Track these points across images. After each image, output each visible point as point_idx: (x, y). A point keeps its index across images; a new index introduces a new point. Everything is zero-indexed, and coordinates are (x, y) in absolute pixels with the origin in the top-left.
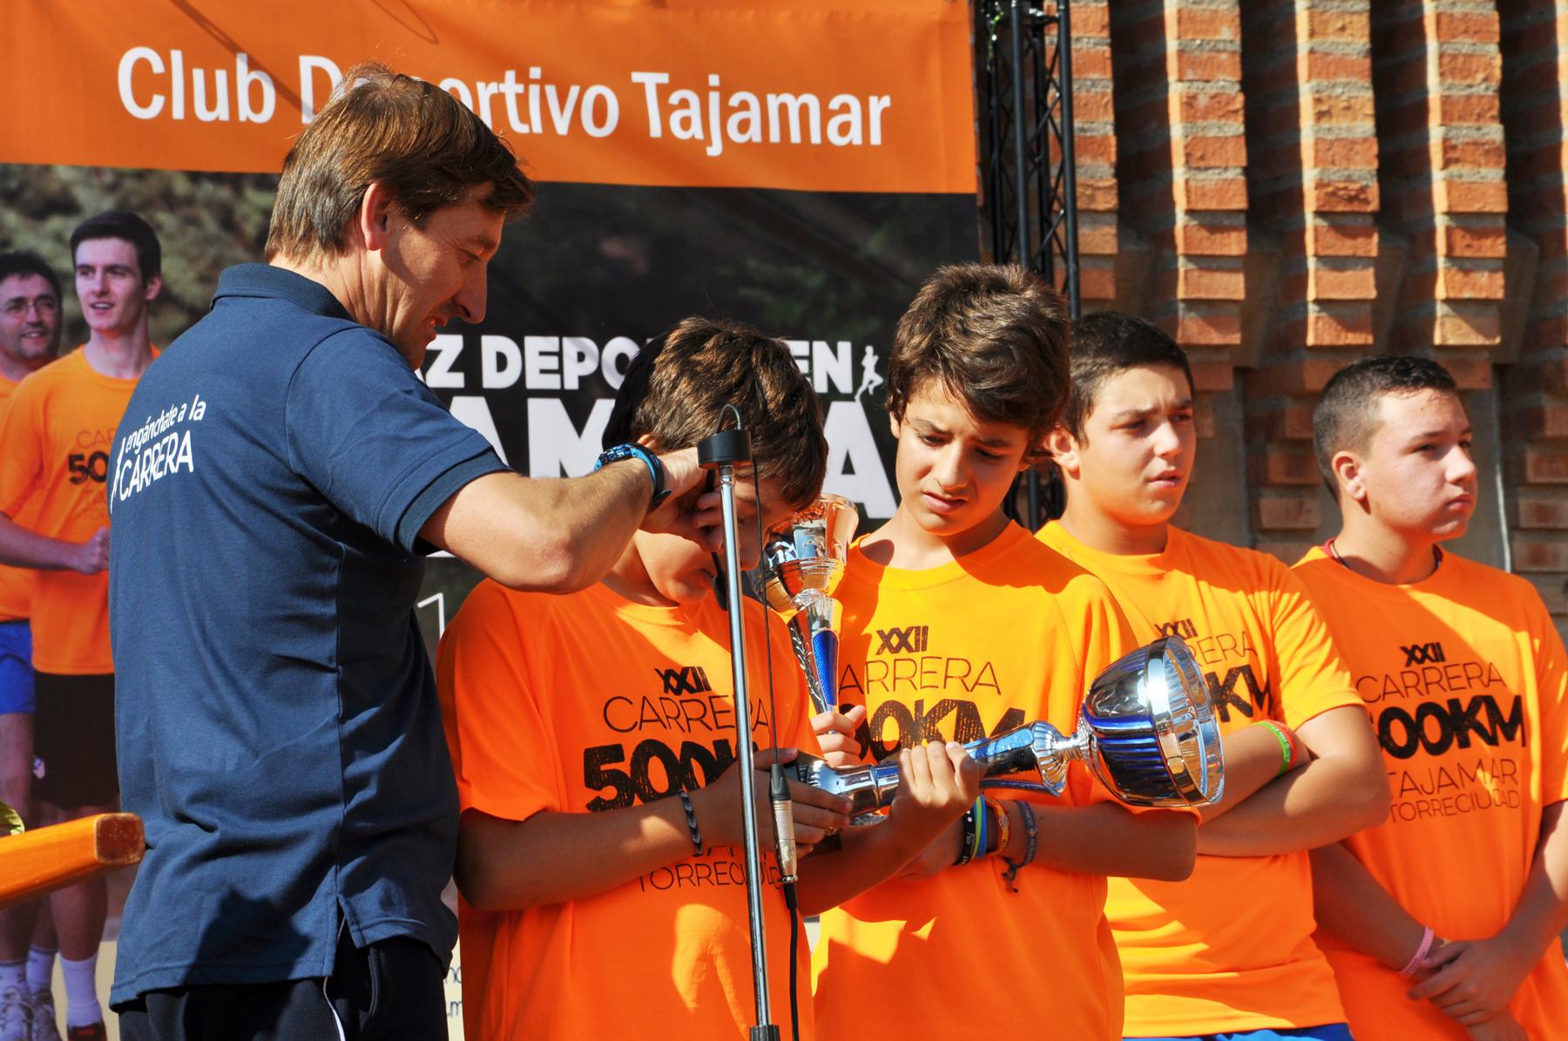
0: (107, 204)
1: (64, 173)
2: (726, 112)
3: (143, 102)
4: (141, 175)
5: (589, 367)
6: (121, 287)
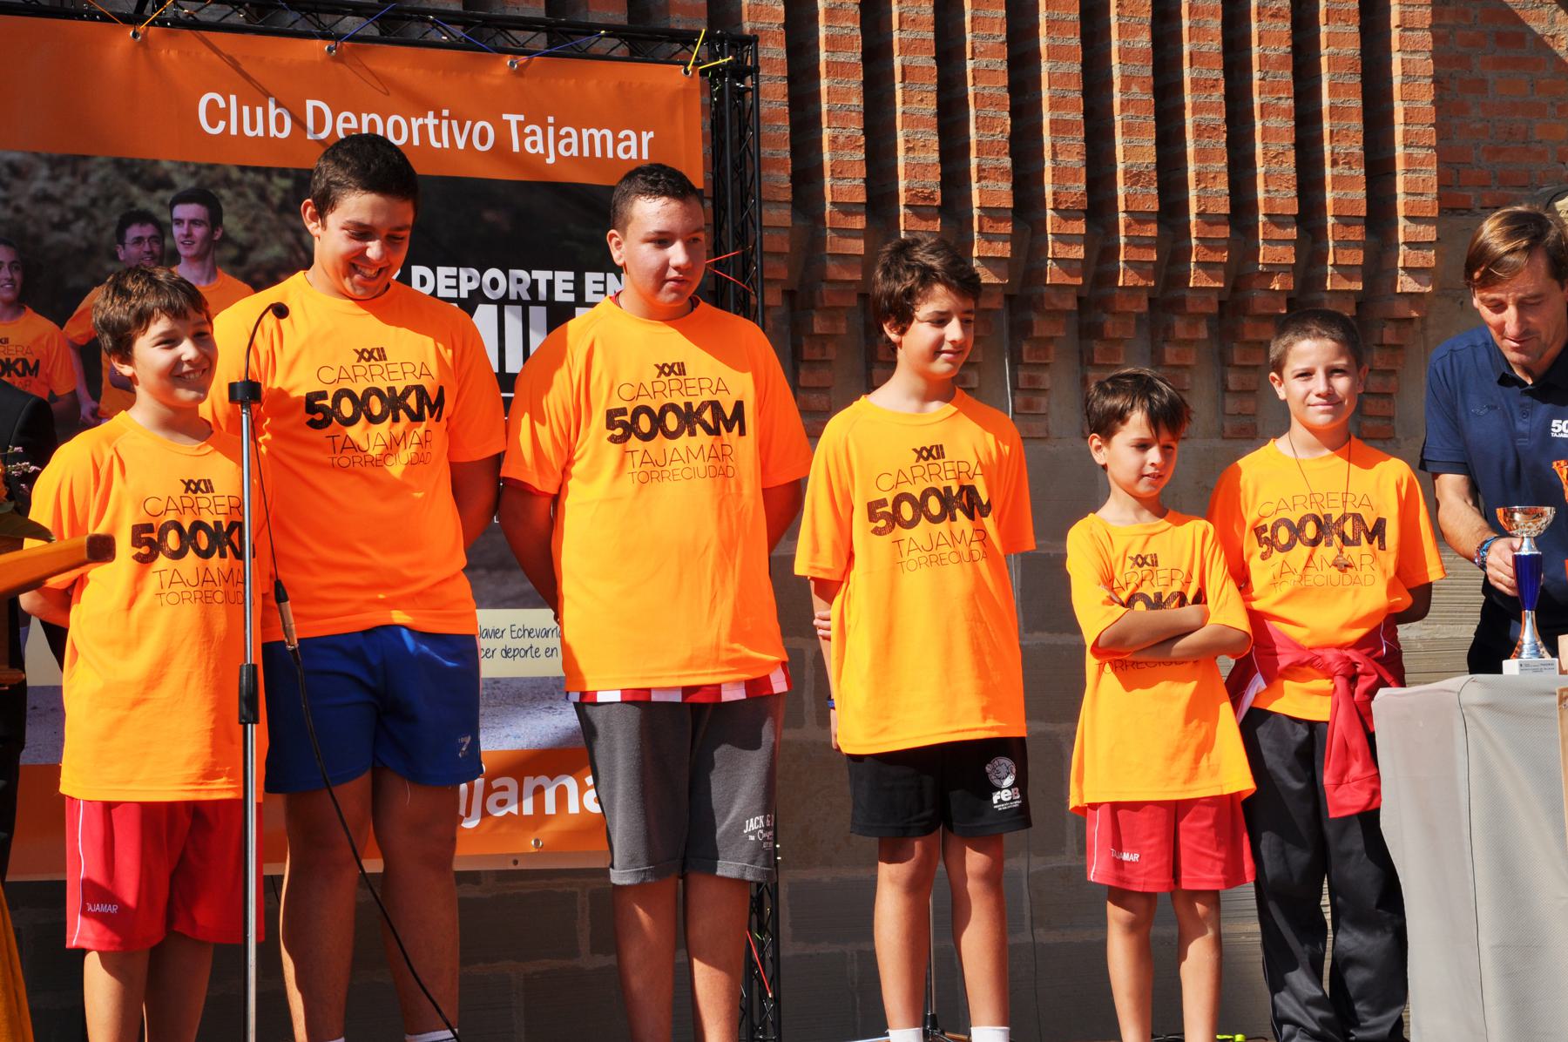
0: (191, 184)
1: (166, 165)
2: (558, 138)
3: (213, 125)
4: (211, 167)
5: (474, 285)
6: (199, 232)
